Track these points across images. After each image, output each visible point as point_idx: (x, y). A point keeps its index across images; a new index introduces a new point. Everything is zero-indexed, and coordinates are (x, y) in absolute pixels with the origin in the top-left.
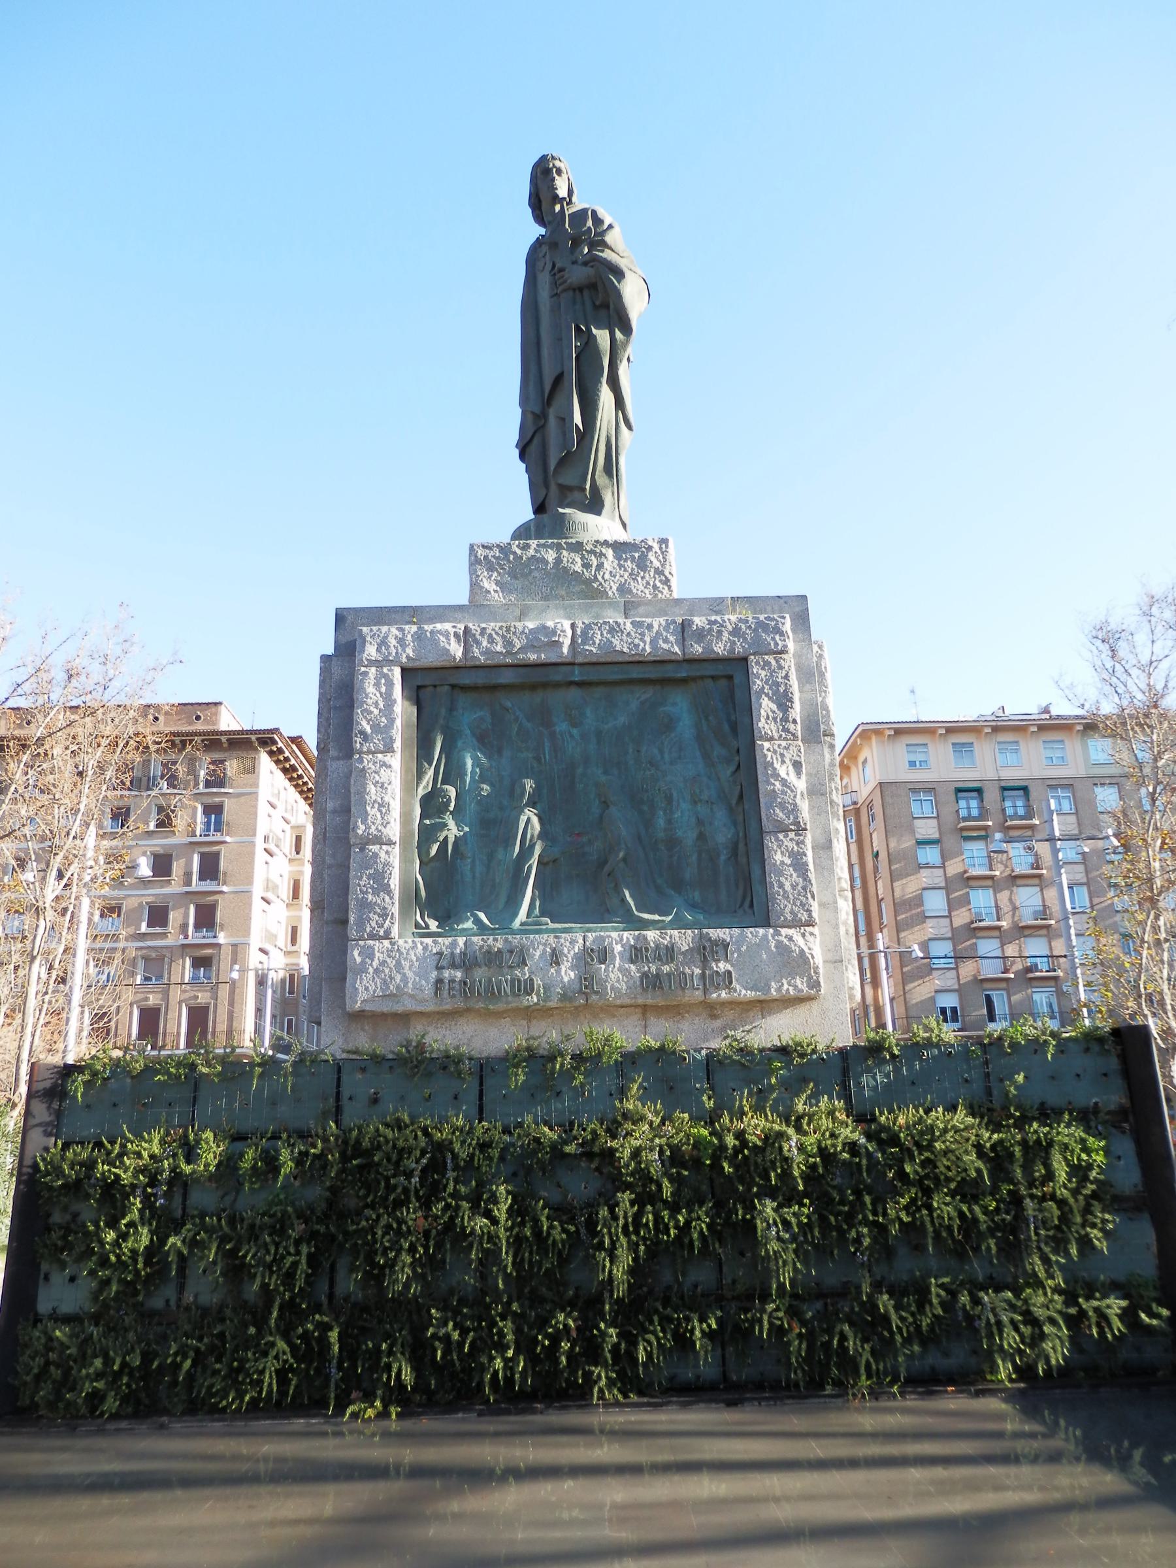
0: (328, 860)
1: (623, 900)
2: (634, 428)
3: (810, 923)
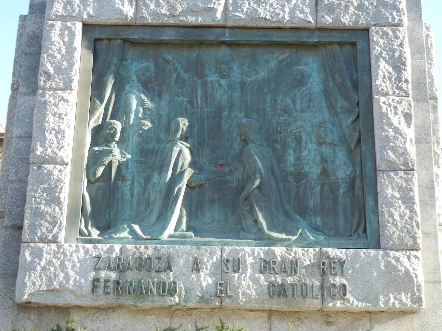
0: (12, 177)
1: (256, 221)
3: (415, 248)
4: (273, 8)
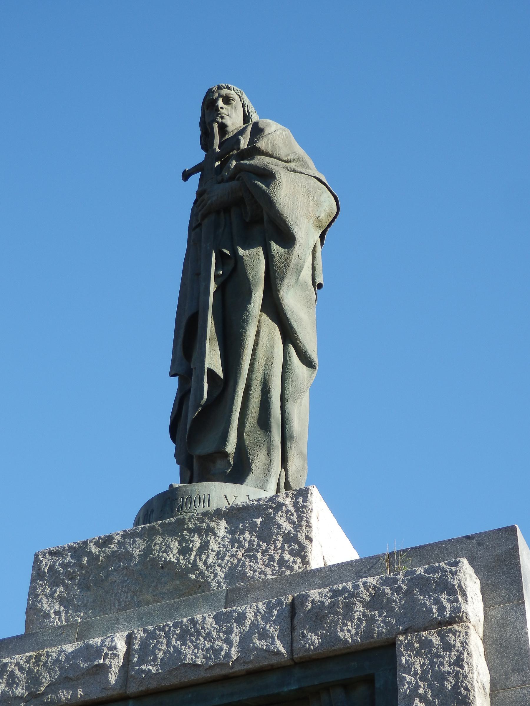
4: (210, 641)
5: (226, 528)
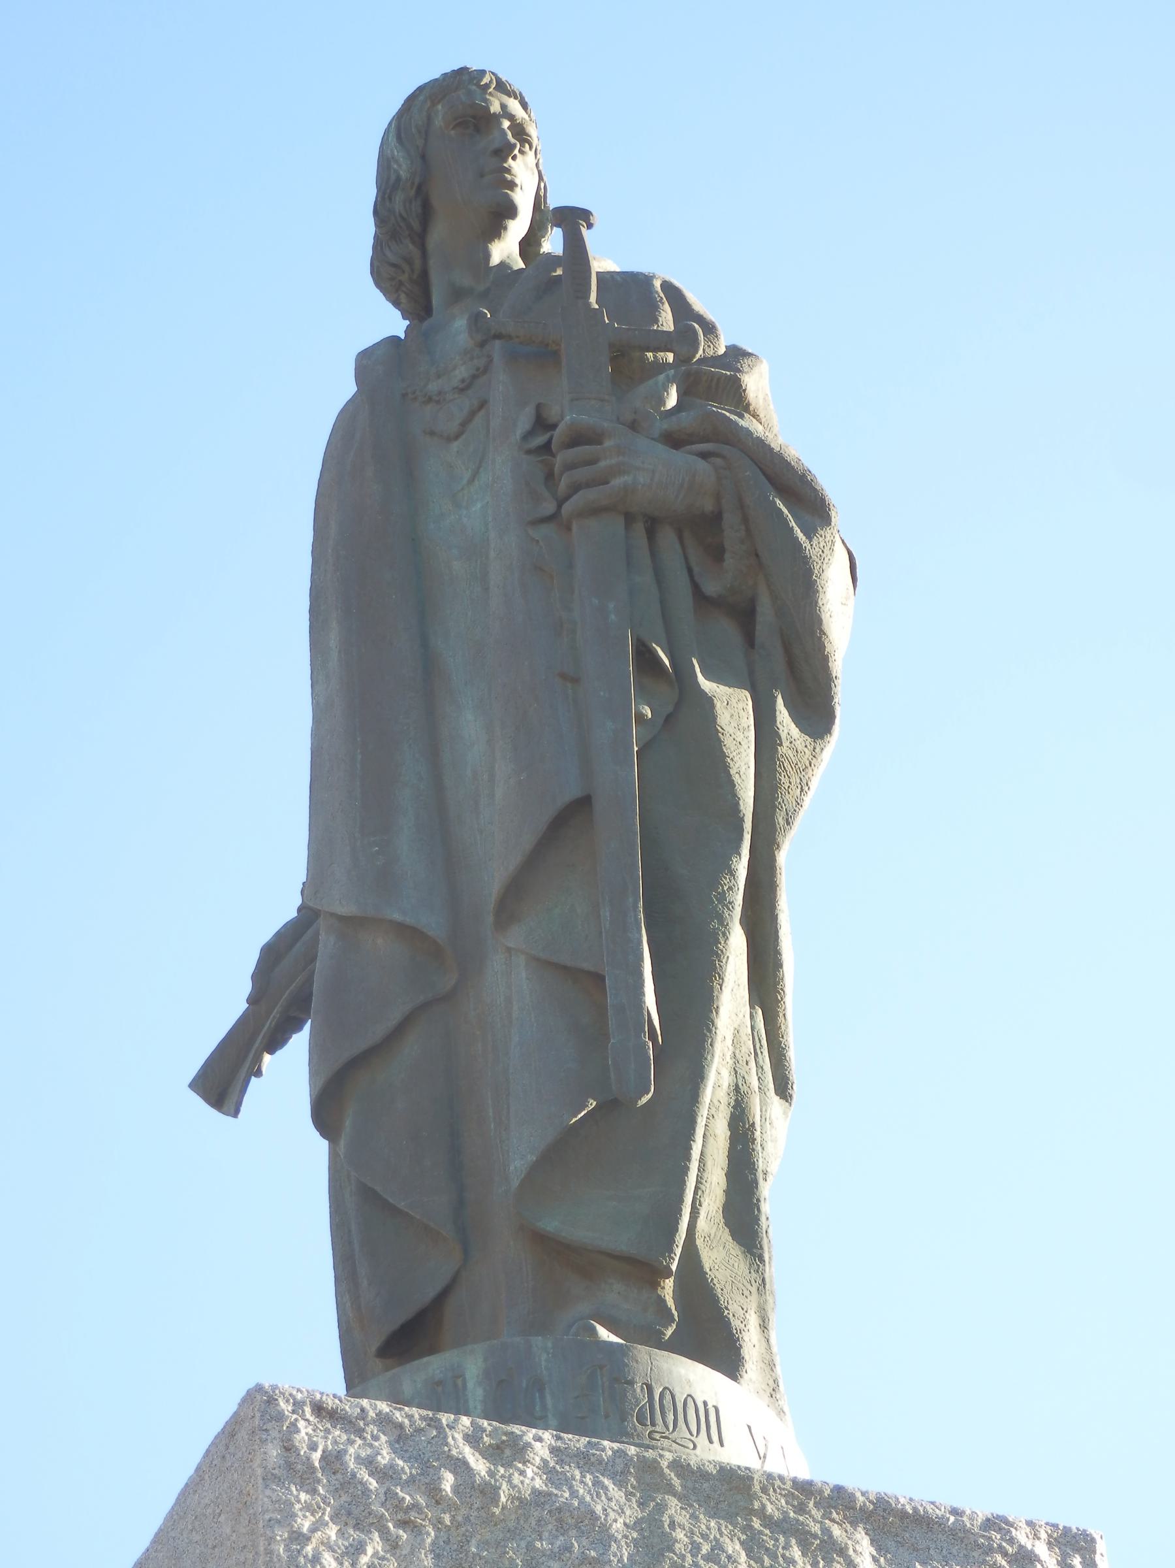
2: (797, 1091)
5: (873, 1557)
